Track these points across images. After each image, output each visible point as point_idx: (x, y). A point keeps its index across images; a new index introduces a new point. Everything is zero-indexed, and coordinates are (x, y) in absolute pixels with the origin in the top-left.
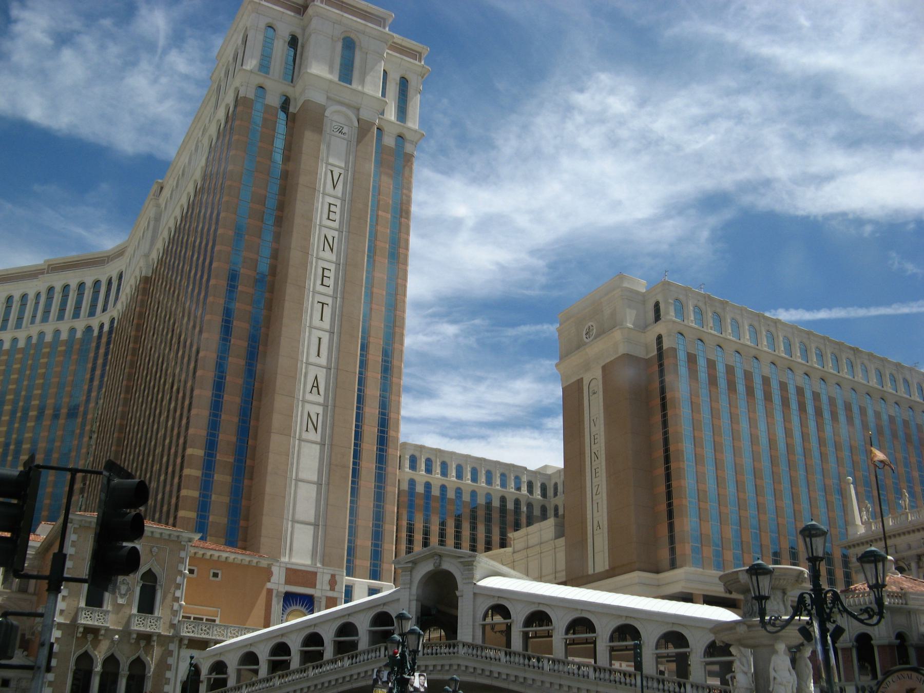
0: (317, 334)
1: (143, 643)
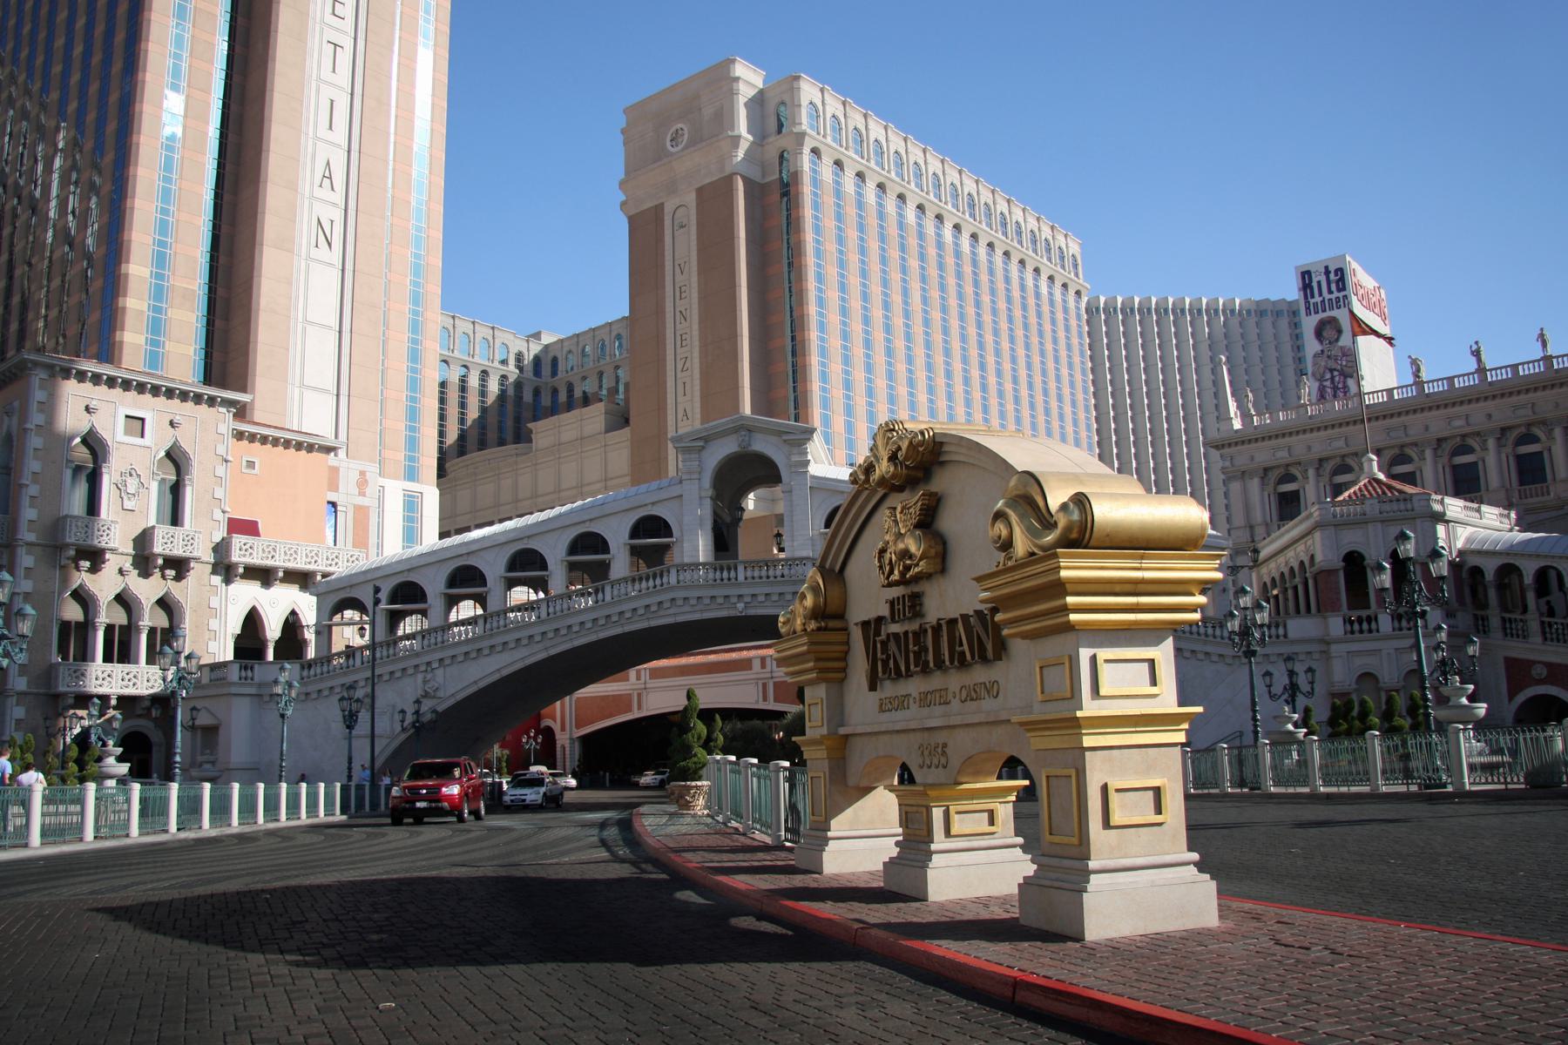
0: (327, 93)
1: (171, 573)
